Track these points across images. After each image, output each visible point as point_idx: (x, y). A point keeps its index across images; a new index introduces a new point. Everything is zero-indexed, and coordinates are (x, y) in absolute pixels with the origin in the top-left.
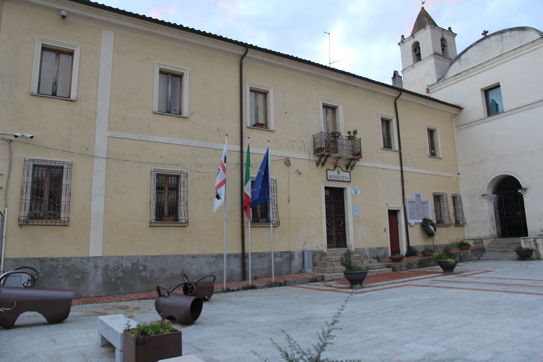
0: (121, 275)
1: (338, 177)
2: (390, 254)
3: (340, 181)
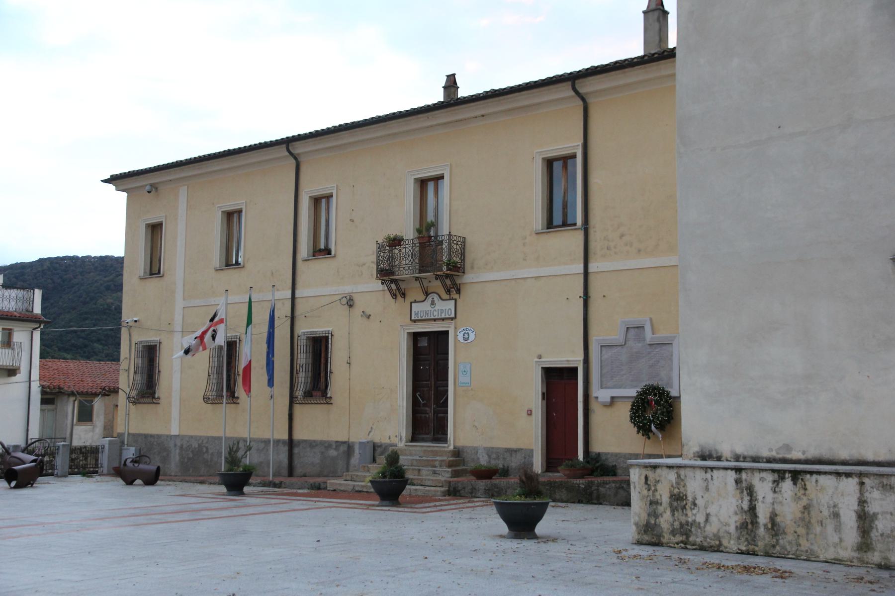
0: (191, 455)
1: (432, 311)
2: (538, 465)
3: (435, 320)
